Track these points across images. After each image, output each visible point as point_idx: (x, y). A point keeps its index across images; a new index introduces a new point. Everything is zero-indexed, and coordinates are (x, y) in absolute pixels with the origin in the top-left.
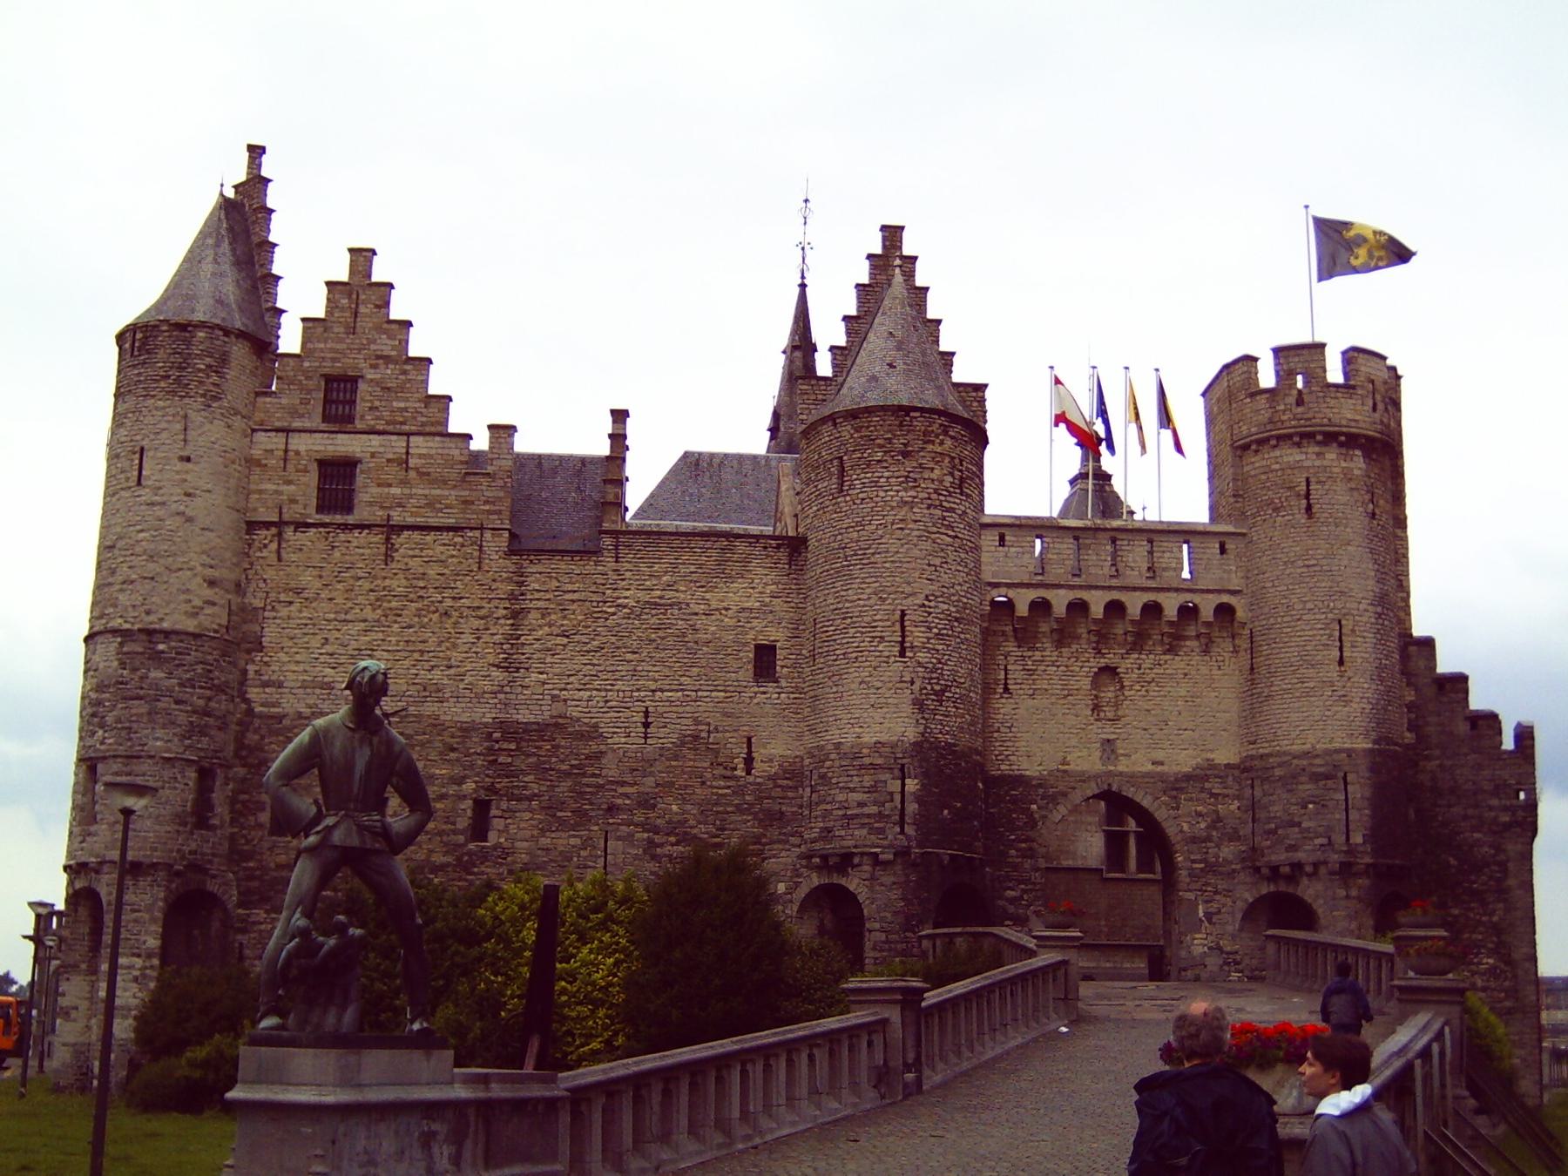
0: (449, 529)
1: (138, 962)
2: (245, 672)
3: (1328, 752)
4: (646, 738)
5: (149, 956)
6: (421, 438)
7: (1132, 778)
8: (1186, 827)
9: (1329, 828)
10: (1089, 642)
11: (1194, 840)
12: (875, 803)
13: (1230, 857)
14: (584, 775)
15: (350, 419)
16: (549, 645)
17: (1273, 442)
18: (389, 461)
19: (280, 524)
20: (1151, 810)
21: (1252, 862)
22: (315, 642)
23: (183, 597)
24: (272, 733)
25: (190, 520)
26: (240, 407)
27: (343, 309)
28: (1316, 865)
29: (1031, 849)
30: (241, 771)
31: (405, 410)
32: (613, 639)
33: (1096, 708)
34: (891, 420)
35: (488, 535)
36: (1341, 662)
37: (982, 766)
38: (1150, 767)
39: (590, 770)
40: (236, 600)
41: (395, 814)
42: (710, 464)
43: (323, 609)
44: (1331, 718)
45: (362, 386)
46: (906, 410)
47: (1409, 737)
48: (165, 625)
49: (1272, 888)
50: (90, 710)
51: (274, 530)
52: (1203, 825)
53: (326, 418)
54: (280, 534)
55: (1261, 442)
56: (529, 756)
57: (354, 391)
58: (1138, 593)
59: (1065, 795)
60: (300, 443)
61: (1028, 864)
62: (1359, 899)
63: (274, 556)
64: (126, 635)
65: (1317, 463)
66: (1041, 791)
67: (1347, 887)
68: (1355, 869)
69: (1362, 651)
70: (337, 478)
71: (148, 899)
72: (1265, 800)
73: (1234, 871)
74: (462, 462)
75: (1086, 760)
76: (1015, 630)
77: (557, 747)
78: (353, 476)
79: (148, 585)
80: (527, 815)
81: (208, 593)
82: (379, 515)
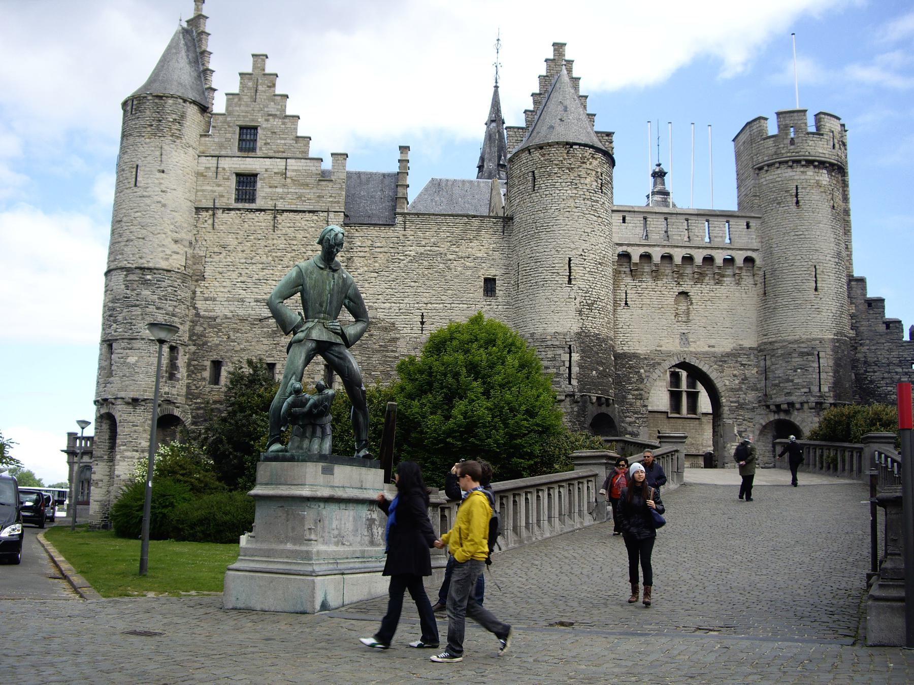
0: (310, 212)
1: (137, 455)
2: (194, 293)
5: (143, 451)
6: (293, 161)
7: (696, 354)
8: (727, 383)
9: (810, 383)
10: (673, 278)
11: (732, 390)
12: (554, 367)
13: (752, 400)
15: (253, 149)
17: (777, 165)
18: (275, 173)
19: (214, 209)
20: (708, 373)
21: (765, 403)
22: (234, 275)
23: (160, 249)
24: (210, 326)
25: (164, 206)
26: (192, 143)
27: (249, 89)
28: (802, 404)
29: (641, 394)
30: (193, 348)
31: (285, 144)
34: (563, 151)
35: (332, 215)
36: (816, 290)
37: (613, 347)
38: (707, 349)
40: (190, 251)
42: (446, 185)
43: (238, 257)
45: (259, 131)
46: (571, 145)
47: (852, 333)
48: (151, 265)
49: (777, 417)
50: (109, 313)
51: (211, 212)
52: (737, 382)
53: (240, 149)
54: (214, 214)
55: (769, 165)
57: (256, 134)
59: (659, 364)
60: (225, 163)
61: (639, 403)
63: (210, 228)
64: (128, 270)
65: (803, 177)
66: (646, 362)
68: (824, 406)
70: (246, 183)
71: (141, 419)
72: (773, 367)
74: (317, 174)
75: (672, 345)
76: (631, 271)
77: (371, 335)
78: (255, 182)
79: (141, 242)
81: (175, 247)
82: (269, 204)
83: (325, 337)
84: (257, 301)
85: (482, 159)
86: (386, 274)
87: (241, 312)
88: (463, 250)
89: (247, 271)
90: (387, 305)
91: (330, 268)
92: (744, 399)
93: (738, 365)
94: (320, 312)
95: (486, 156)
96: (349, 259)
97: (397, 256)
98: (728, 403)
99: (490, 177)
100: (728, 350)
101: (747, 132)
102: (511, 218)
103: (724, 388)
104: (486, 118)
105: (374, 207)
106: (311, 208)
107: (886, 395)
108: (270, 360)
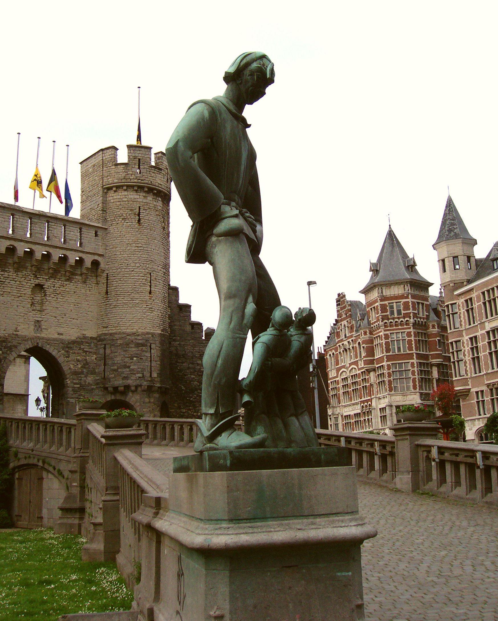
3: (143, 334)
7: (48, 341)
9: (144, 370)
10: (31, 270)
11: (75, 373)
13: (91, 382)
17: (125, 188)
20: (57, 357)
28: (136, 387)
33: (33, 304)
36: (150, 293)
38: (56, 336)
44: (142, 320)
49: (113, 397)
52: (80, 366)
58: (58, 250)
59: (16, 347)
62: (154, 403)
66: (4, 344)
67: (149, 397)
68: (153, 389)
69: (159, 290)
72: (113, 355)
73: (93, 389)
75: (27, 330)
92: (85, 382)
93: (81, 351)
98: (72, 385)
100: (73, 338)
101: (99, 157)
103: (69, 371)
107: (191, 381)
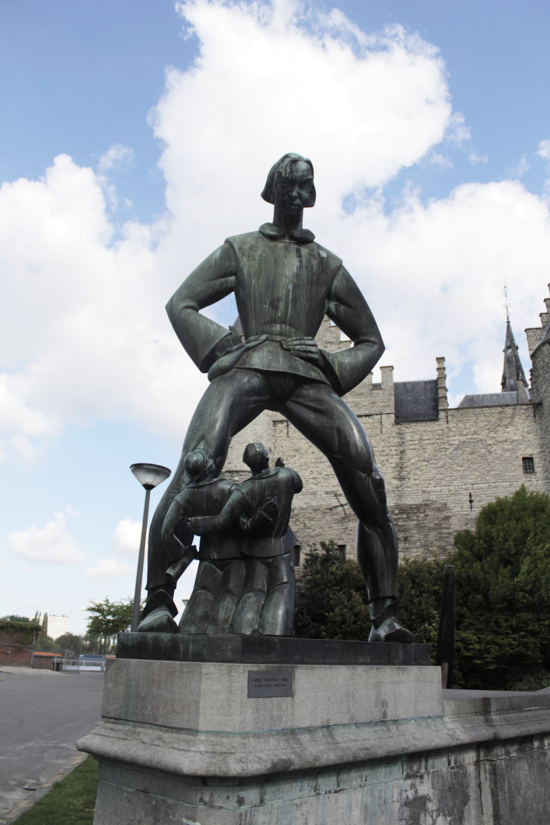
0: (366, 416)
4: (471, 508)
14: (442, 528)
16: (418, 466)
32: (450, 461)
35: (384, 417)
39: (444, 526)
41: (350, 553)
42: (478, 399)
56: (413, 520)
63: (286, 435)
77: (426, 516)
80: (415, 550)
83: (281, 364)
84: (327, 493)
85: (504, 378)
86: (435, 461)
87: (314, 504)
88: (501, 435)
89: (317, 469)
90: (438, 488)
91: (292, 238)
94: (273, 321)
95: (507, 375)
96: (402, 452)
97: (443, 446)
99: (512, 389)
102: (540, 404)
104: (503, 346)
105: (419, 408)
106: (367, 412)
108: (340, 543)
